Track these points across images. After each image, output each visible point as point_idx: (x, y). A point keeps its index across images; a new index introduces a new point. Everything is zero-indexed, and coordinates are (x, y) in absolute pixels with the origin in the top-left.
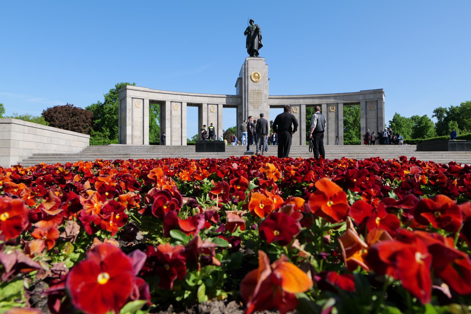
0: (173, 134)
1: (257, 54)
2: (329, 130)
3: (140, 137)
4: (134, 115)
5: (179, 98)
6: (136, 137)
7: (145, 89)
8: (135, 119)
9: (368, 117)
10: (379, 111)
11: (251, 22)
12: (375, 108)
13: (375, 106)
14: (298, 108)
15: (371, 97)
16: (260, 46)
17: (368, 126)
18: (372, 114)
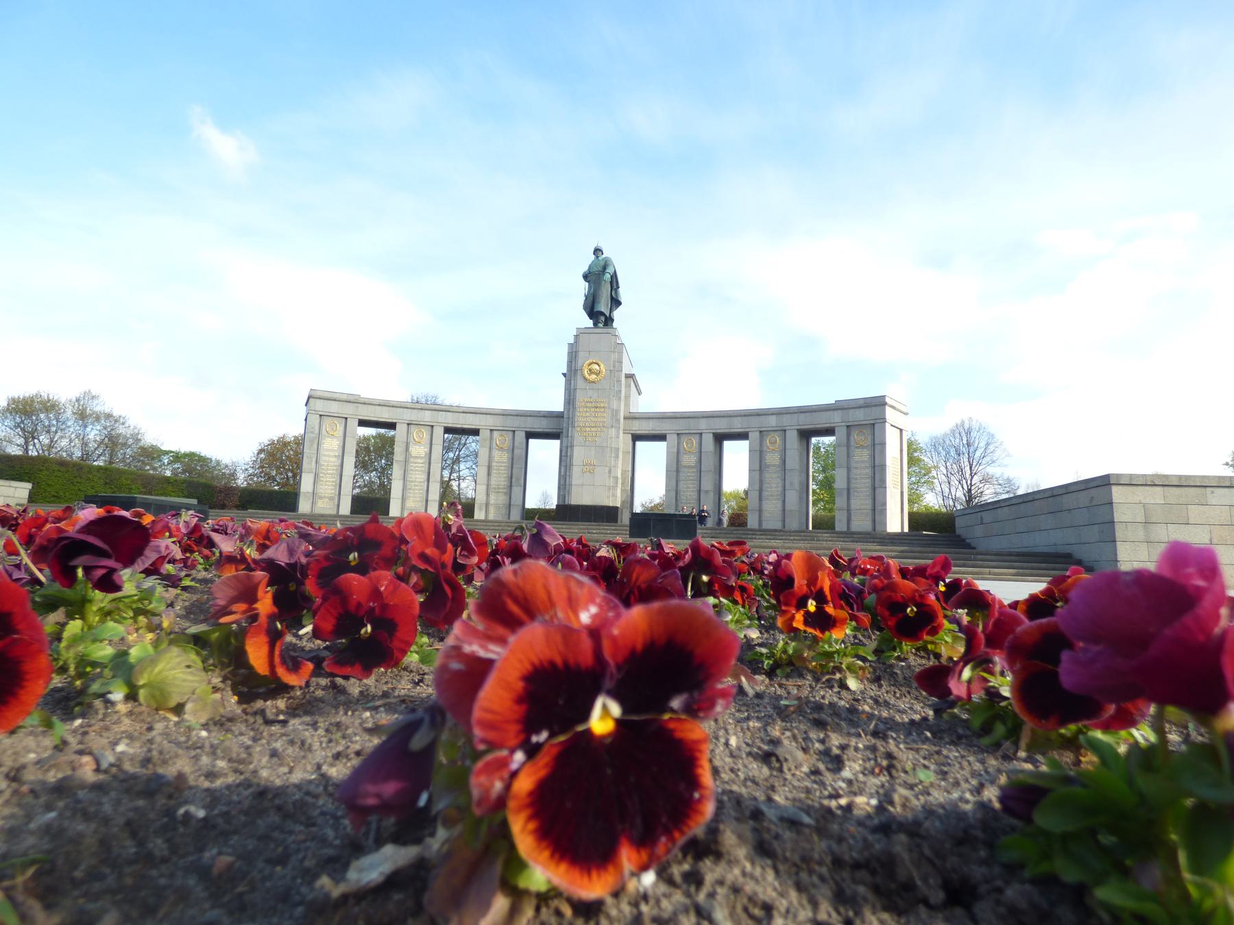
0: (410, 494)
1: (609, 321)
2: (765, 494)
3: (331, 499)
4: (322, 452)
5: (427, 417)
6: (321, 498)
7: (352, 399)
8: (323, 460)
9: (853, 465)
10: (878, 448)
11: (597, 251)
12: (869, 442)
13: (870, 437)
14: (695, 441)
15: (859, 416)
16: (616, 302)
17: (852, 486)
18: (862, 457)
